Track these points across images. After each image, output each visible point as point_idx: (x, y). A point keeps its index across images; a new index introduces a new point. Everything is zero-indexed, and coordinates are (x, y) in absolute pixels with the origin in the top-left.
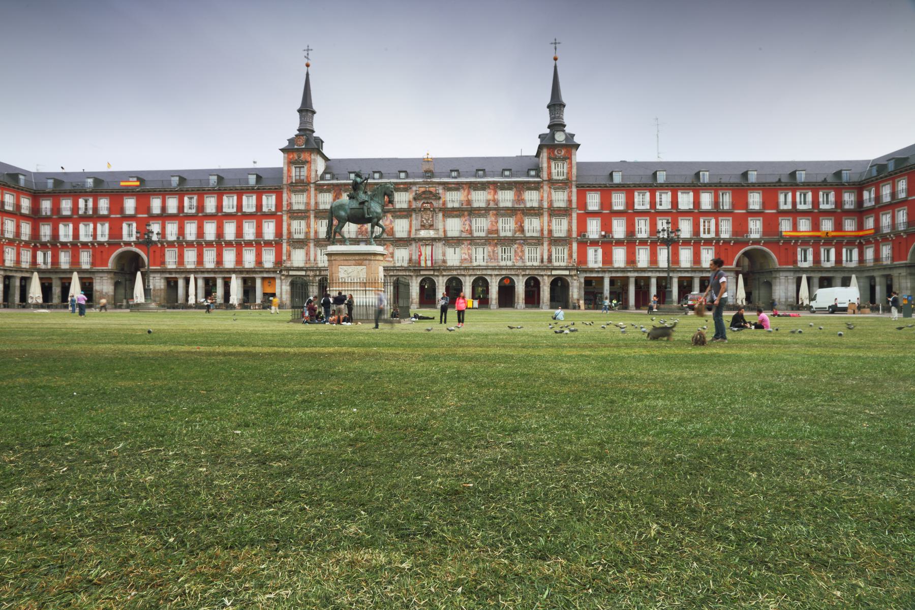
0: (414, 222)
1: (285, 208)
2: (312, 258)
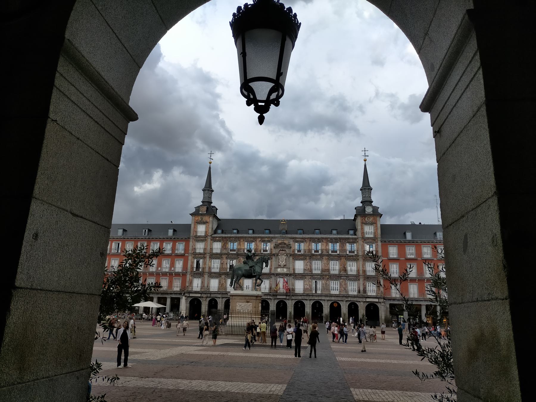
0: (274, 263)
1: (190, 252)
2: (206, 285)
